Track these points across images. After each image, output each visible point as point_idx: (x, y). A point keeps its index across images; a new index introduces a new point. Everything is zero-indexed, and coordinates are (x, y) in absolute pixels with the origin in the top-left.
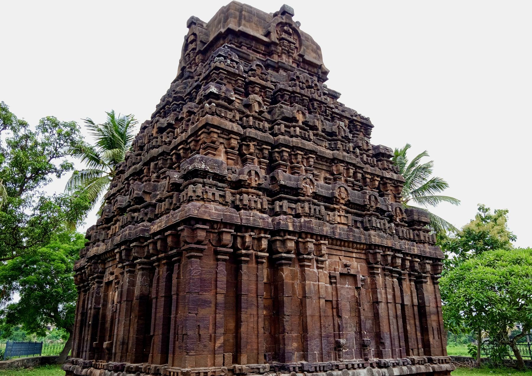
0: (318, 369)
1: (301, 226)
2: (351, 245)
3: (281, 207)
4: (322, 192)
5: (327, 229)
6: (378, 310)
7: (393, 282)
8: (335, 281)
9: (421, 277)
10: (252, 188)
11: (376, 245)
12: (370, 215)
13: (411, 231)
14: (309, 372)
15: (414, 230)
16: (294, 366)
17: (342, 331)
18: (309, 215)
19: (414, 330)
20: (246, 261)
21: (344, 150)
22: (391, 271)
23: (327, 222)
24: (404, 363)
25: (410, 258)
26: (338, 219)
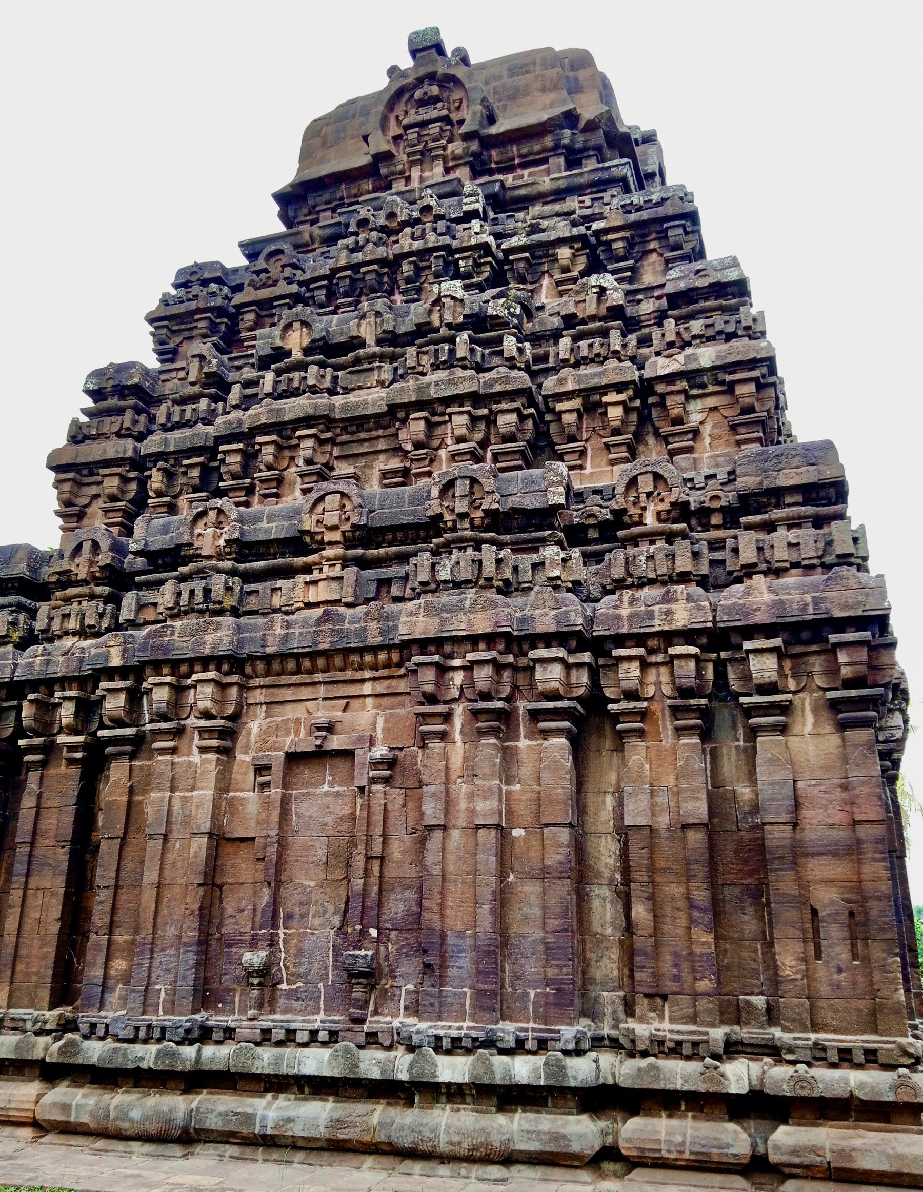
0: (142, 1034)
4: (266, 531)
10: (78, 583)
16: (94, 1020)
20: (38, 762)
21: (436, 367)
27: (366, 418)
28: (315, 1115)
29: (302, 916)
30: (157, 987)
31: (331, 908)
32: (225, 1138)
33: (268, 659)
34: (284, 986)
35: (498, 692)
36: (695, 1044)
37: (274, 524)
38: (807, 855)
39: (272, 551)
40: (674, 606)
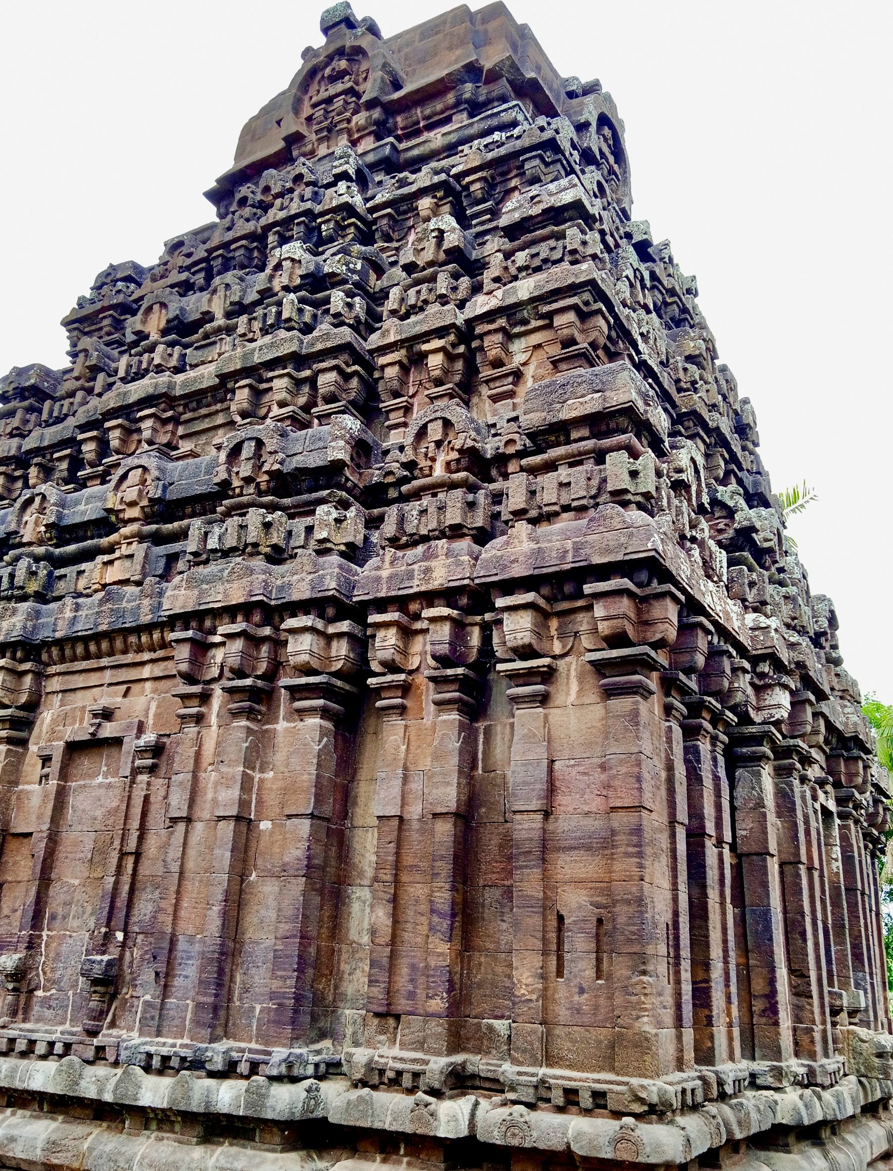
21: (265, 331)
27: (202, 392)
29: (64, 918)
31: (89, 909)
33: (60, 643)
34: (39, 993)
35: (254, 669)
36: (416, 1075)
37: (90, 506)
38: (558, 849)
40: (433, 563)
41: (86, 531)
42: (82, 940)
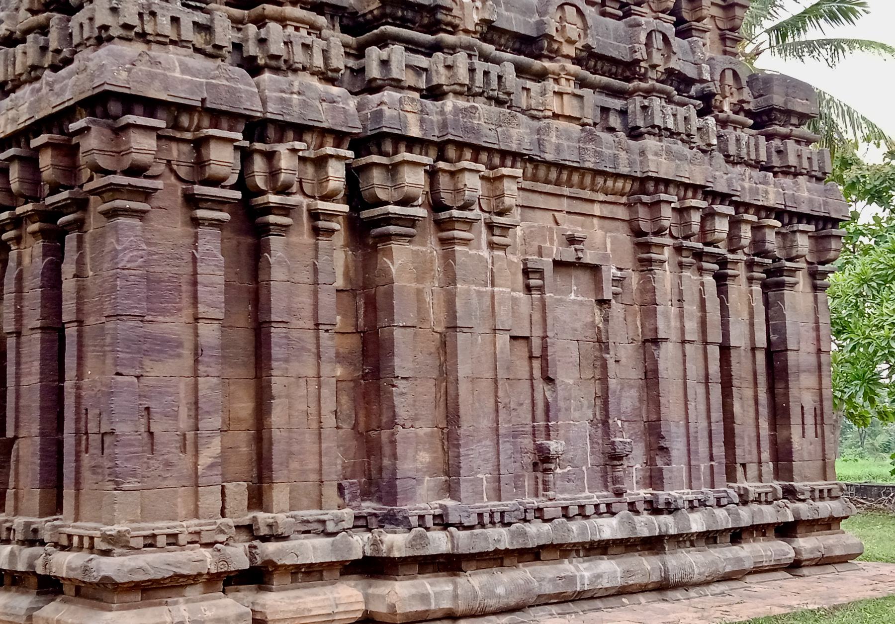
0: (486, 519)
1: (444, 125)
2: (588, 180)
3: (385, 63)
4: (509, 20)
5: (519, 135)
6: (656, 363)
7: (702, 284)
8: (539, 282)
9: (780, 271)
11: (658, 181)
12: (648, 93)
13: (762, 139)
14: (461, 526)
15: (769, 137)
16: (422, 513)
17: (556, 419)
18: (468, 92)
19: (752, 413)
22: (699, 255)
23: (523, 112)
24: (718, 500)
25: (754, 218)
26: (555, 105)
28: (609, 570)
30: (480, 476)
31: (585, 403)
32: (544, 601)
39: (503, 41)
41: (500, 37)
42: (584, 428)
